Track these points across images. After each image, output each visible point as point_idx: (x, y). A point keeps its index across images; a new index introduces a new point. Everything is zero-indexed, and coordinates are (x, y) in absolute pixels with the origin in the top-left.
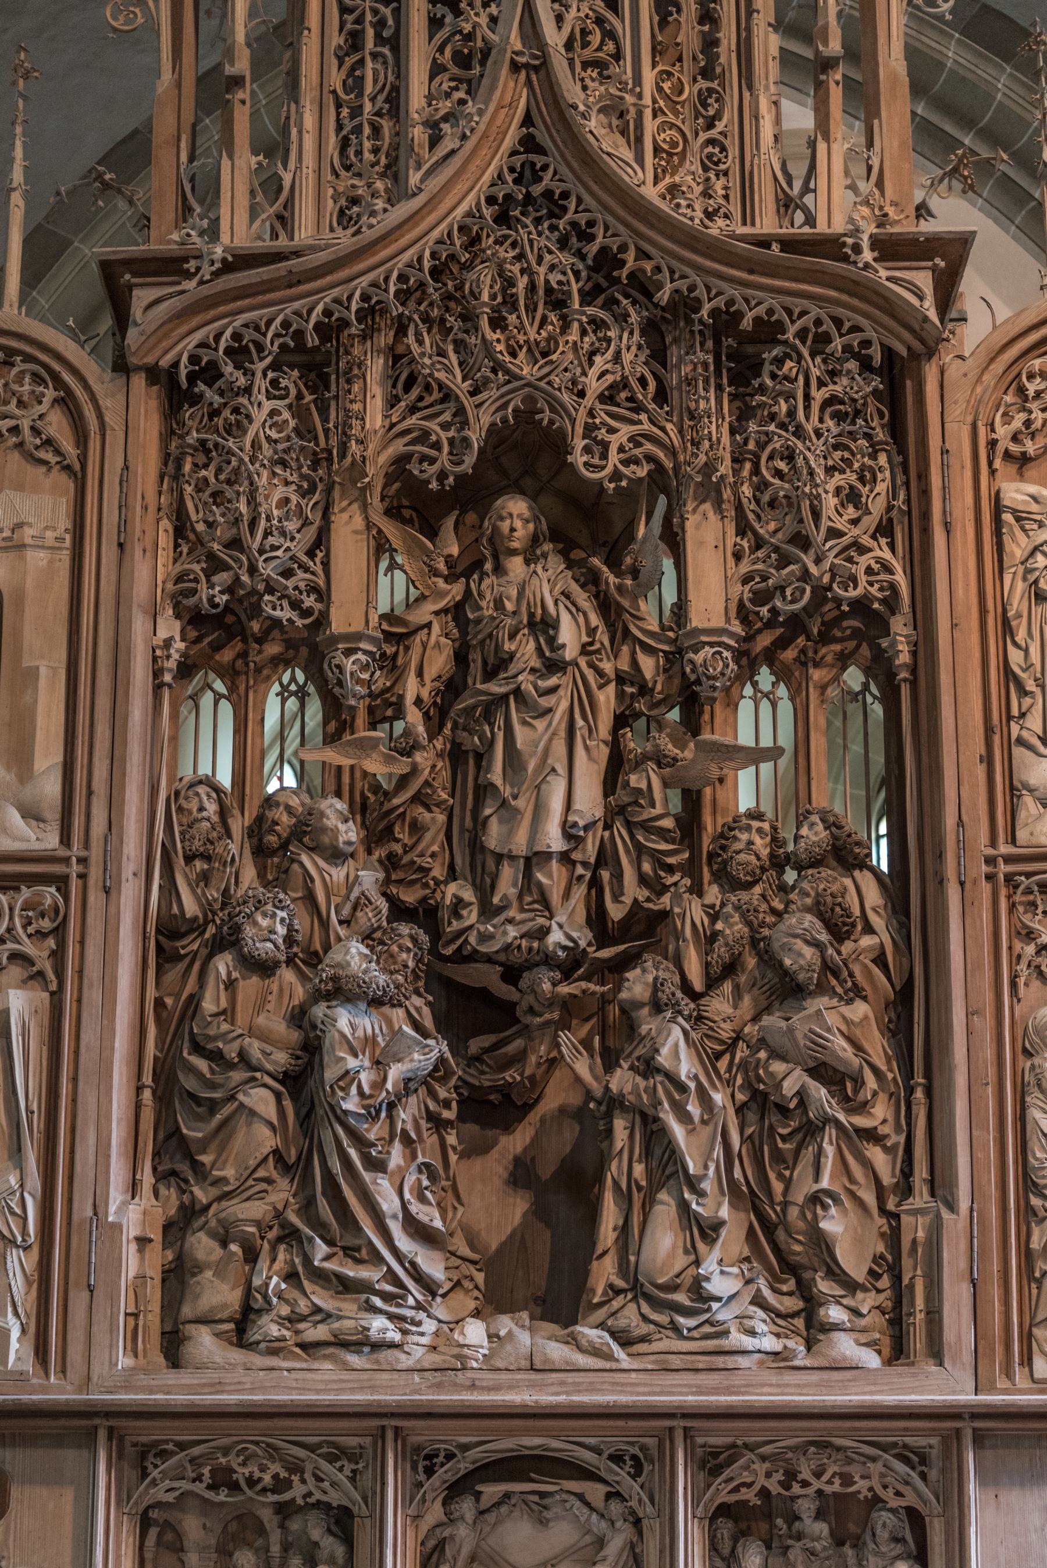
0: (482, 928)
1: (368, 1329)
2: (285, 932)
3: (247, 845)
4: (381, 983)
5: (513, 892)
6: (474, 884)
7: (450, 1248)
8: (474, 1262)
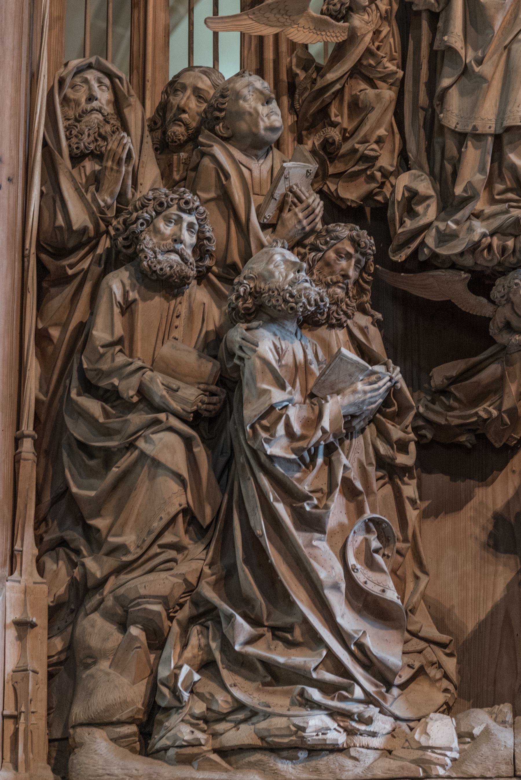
0: (442, 226)
1: (303, 729)
2: (194, 240)
3: (148, 140)
4: (313, 296)
5: (479, 179)
6: (432, 174)
7: (410, 628)
8: (442, 645)
